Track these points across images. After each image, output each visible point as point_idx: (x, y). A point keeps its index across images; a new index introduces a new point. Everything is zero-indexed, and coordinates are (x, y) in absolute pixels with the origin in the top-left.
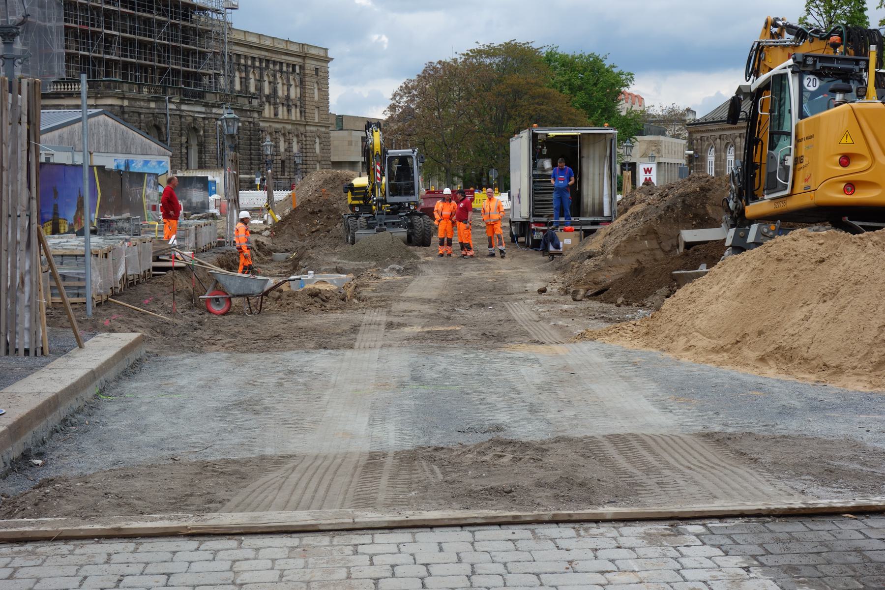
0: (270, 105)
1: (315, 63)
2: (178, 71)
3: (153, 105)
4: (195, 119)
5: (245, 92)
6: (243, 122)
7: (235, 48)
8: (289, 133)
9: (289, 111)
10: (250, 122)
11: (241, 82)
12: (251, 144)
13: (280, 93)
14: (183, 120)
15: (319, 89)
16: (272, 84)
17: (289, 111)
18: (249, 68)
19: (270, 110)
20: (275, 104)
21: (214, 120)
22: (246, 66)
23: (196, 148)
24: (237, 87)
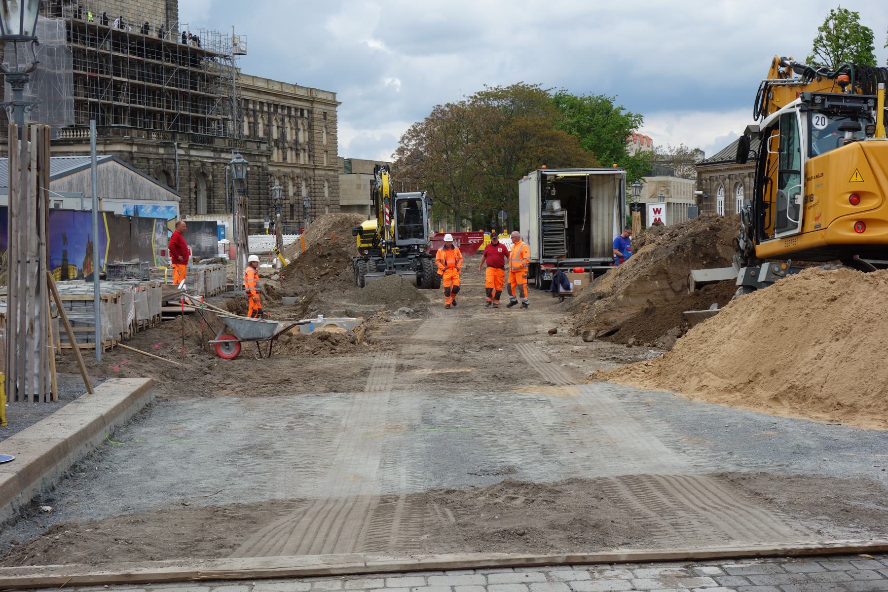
0: (278, 149)
1: (323, 107)
2: (187, 117)
3: (161, 151)
4: (203, 164)
5: (253, 138)
6: (252, 167)
7: (243, 93)
8: (298, 177)
9: (297, 155)
10: (259, 167)
11: (250, 127)
12: (259, 188)
13: (289, 138)
14: (192, 165)
15: (327, 133)
16: (281, 129)
17: (297, 155)
18: (258, 113)
19: (278, 154)
20: (284, 148)
21: (222, 165)
22: (254, 111)
23: (205, 193)
24: (246, 132)
